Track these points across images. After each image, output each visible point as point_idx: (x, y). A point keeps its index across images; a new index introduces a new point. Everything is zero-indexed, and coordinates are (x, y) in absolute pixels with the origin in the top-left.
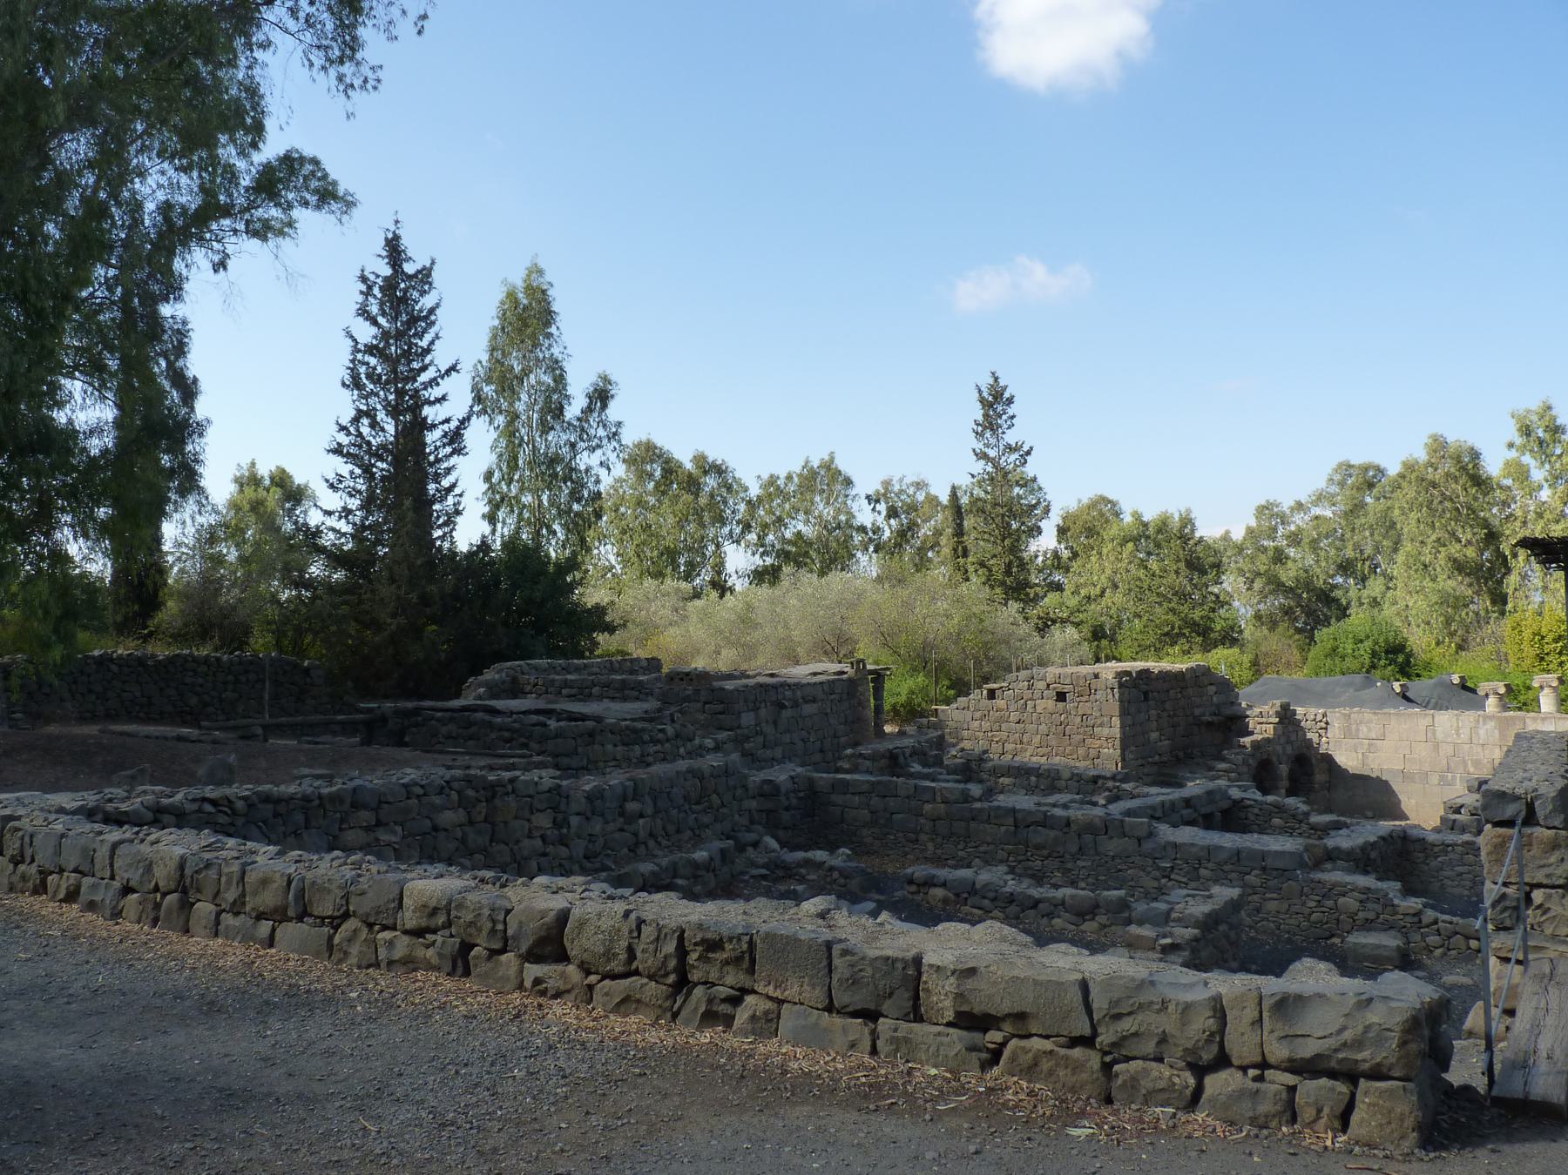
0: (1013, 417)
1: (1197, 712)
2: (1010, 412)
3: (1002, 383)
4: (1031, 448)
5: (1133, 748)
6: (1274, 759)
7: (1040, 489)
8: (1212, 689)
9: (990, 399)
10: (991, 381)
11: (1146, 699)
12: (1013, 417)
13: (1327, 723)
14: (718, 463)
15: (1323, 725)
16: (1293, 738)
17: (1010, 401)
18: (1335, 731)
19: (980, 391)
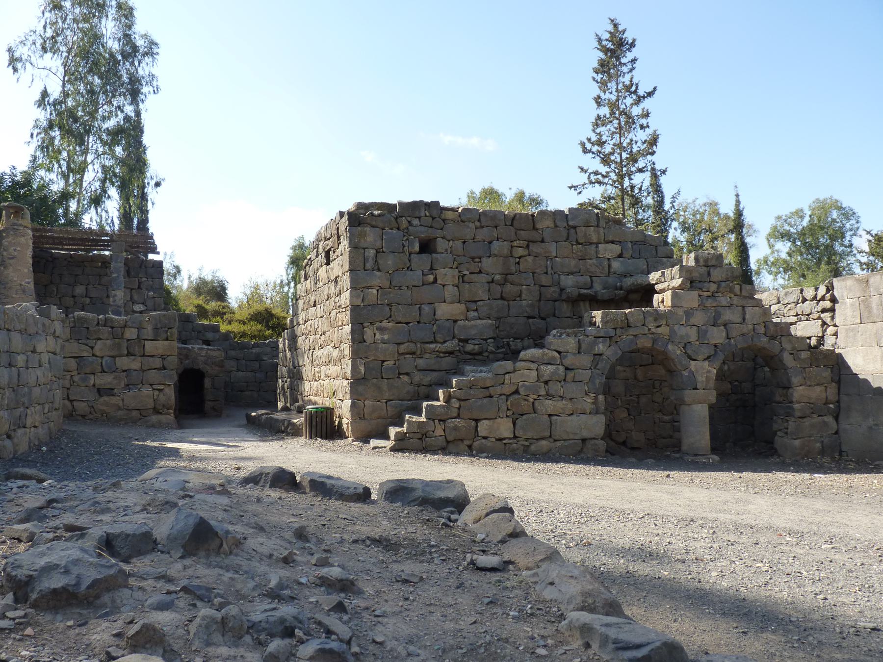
0: (634, 60)
2: (630, 56)
3: (621, 28)
4: (655, 89)
5: (385, 324)
6: (676, 351)
7: (854, 213)
8: (609, 251)
9: (610, 45)
10: (611, 28)
11: (427, 247)
12: (634, 60)
13: (834, 300)
14: (535, 196)
15: (827, 304)
16: (728, 315)
17: (633, 45)
18: (845, 313)
19: (600, 40)
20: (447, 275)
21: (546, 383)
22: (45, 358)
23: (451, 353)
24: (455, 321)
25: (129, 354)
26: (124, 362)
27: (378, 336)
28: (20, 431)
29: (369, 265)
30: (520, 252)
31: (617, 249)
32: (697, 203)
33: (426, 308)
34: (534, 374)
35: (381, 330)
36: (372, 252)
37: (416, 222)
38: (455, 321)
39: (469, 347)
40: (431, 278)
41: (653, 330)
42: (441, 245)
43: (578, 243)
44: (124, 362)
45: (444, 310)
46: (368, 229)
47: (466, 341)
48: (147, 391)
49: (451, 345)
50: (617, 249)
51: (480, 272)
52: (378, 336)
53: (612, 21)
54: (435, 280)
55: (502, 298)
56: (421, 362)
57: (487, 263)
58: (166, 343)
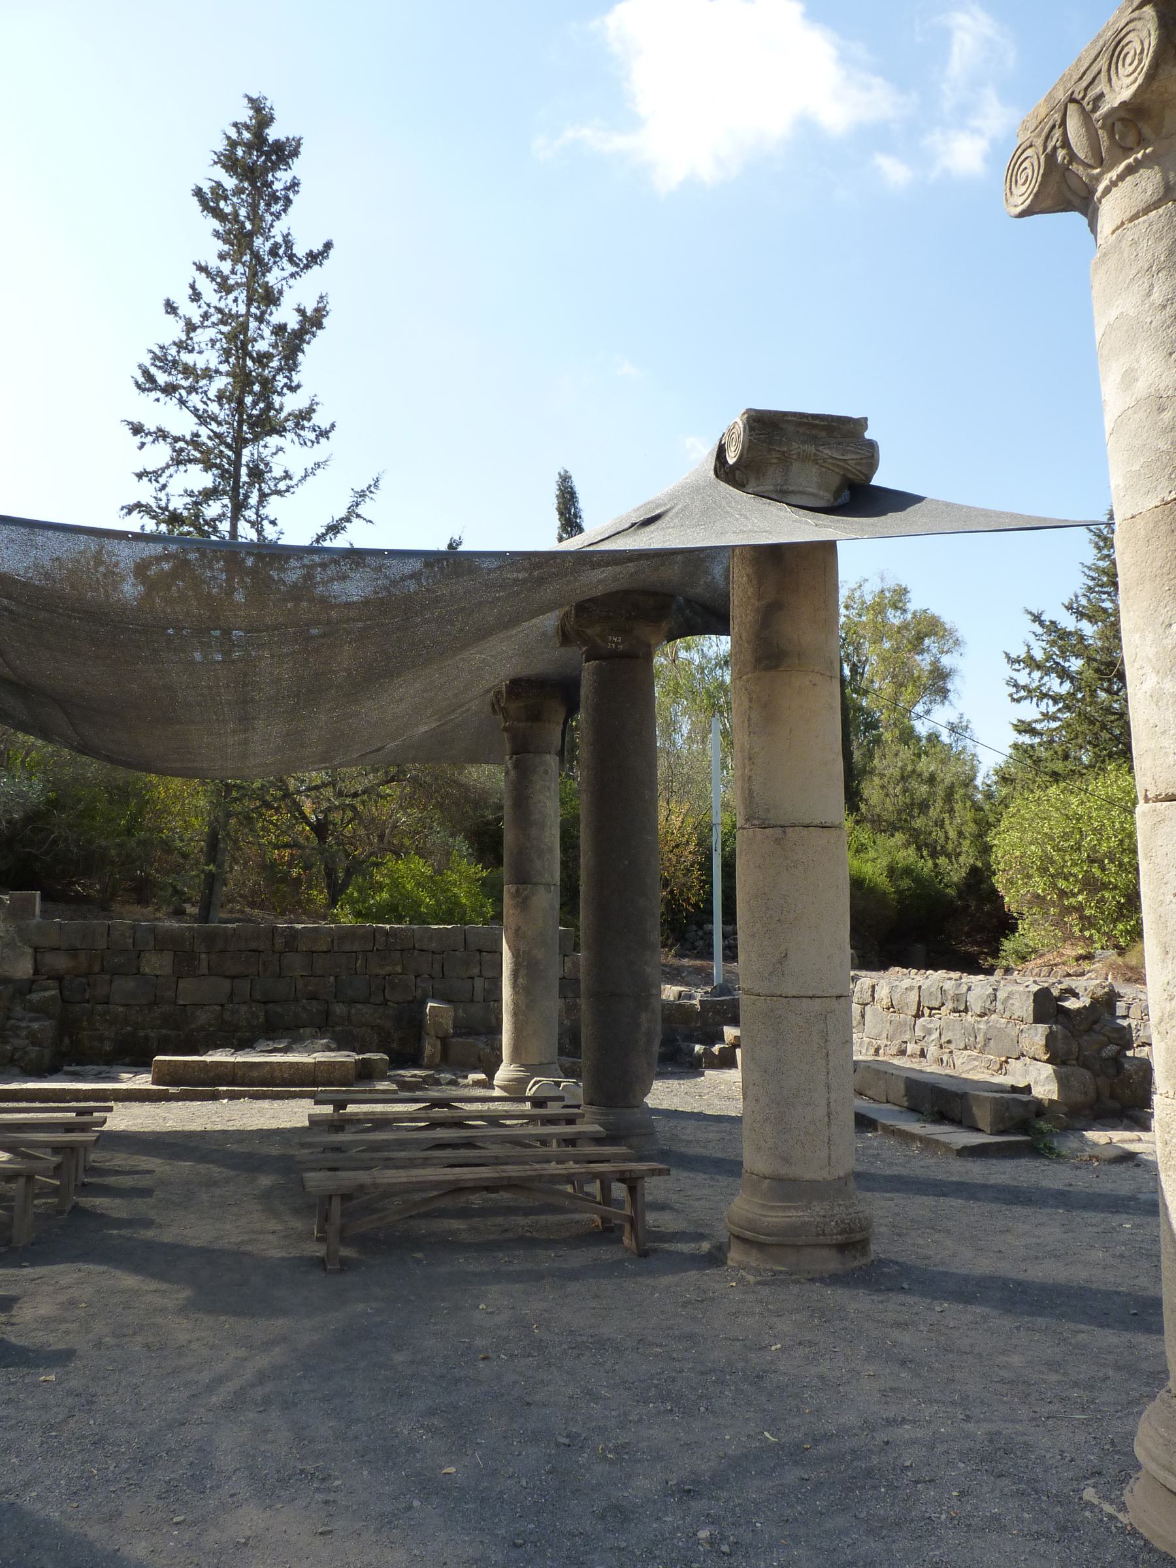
0: (294, 185)
4: (328, 246)
12: (294, 185)
17: (295, 153)
32: (867, 588)
53: (251, 100)
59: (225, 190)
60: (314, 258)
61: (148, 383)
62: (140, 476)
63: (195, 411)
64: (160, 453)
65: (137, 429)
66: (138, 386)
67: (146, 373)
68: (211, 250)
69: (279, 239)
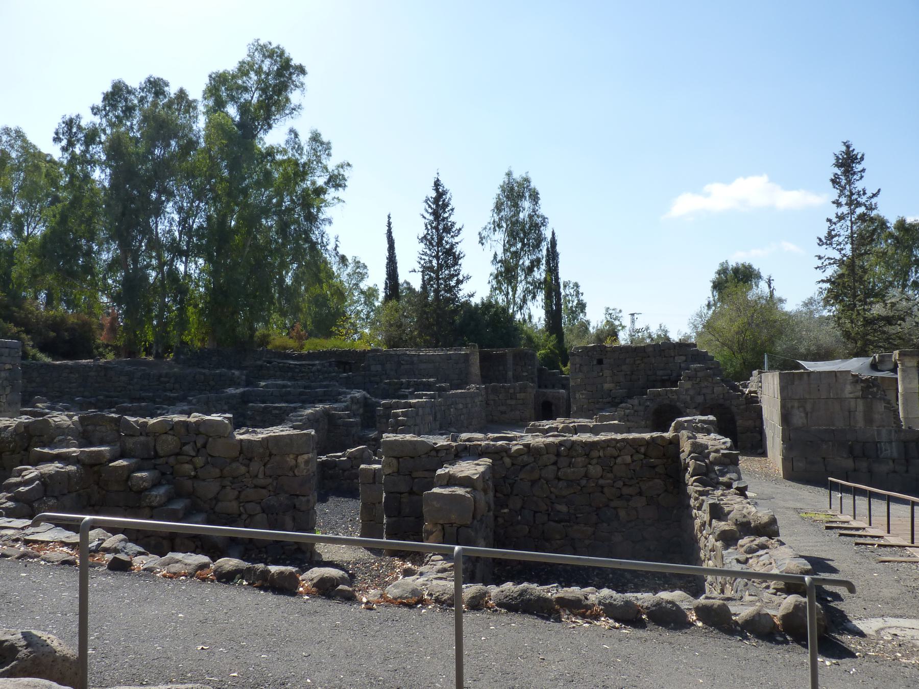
0: (863, 170)
1: (660, 373)
4: (879, 191)
5: (584, 392)
10: (844, 149)
11: (600, 362)
12: (863, 170)
17: (862, 158)
20: (607, 373)
21: (628, 416)
22: (479, 403)
23: (609, 403)
24: (611, 390)
25: (511, 398)
26: (509, 402)
27: (581, 396)
28: (471, 426)
29: (577, 370)
30: (638, 362)
31: (683, 358)
33: (599, 386)
34: (623, 413)
35: (582, 394)
36: (578, 365)
37: (595, 353)
38: (611, 390)
39: (616, 400)
40: (601, 374)
41: (670, 397)
42: (605, 361)
43: (665, 357)
44: (509, 402)
45: (607, 386)
46: (576, 357)
47: (615, 398)
48: (518, 412)
49: (609, 399)
50: (683, 358)
51: (621, 371)
52: (581, 396)
53: (845, 143)
54: (603, 375)
55: (631, 381)
56: (597, 406)
57: (624, 367)
58: (524, 394)
59: (838, 175)
60: (874, 195)
61: (821, 242)
62: (816, 268)
63: (838, 250)
64: (827, 262)
65: (820, 258)
66: (819, 244)
67: (820, 240)
68: (834, 193)
69: (860, 189)
